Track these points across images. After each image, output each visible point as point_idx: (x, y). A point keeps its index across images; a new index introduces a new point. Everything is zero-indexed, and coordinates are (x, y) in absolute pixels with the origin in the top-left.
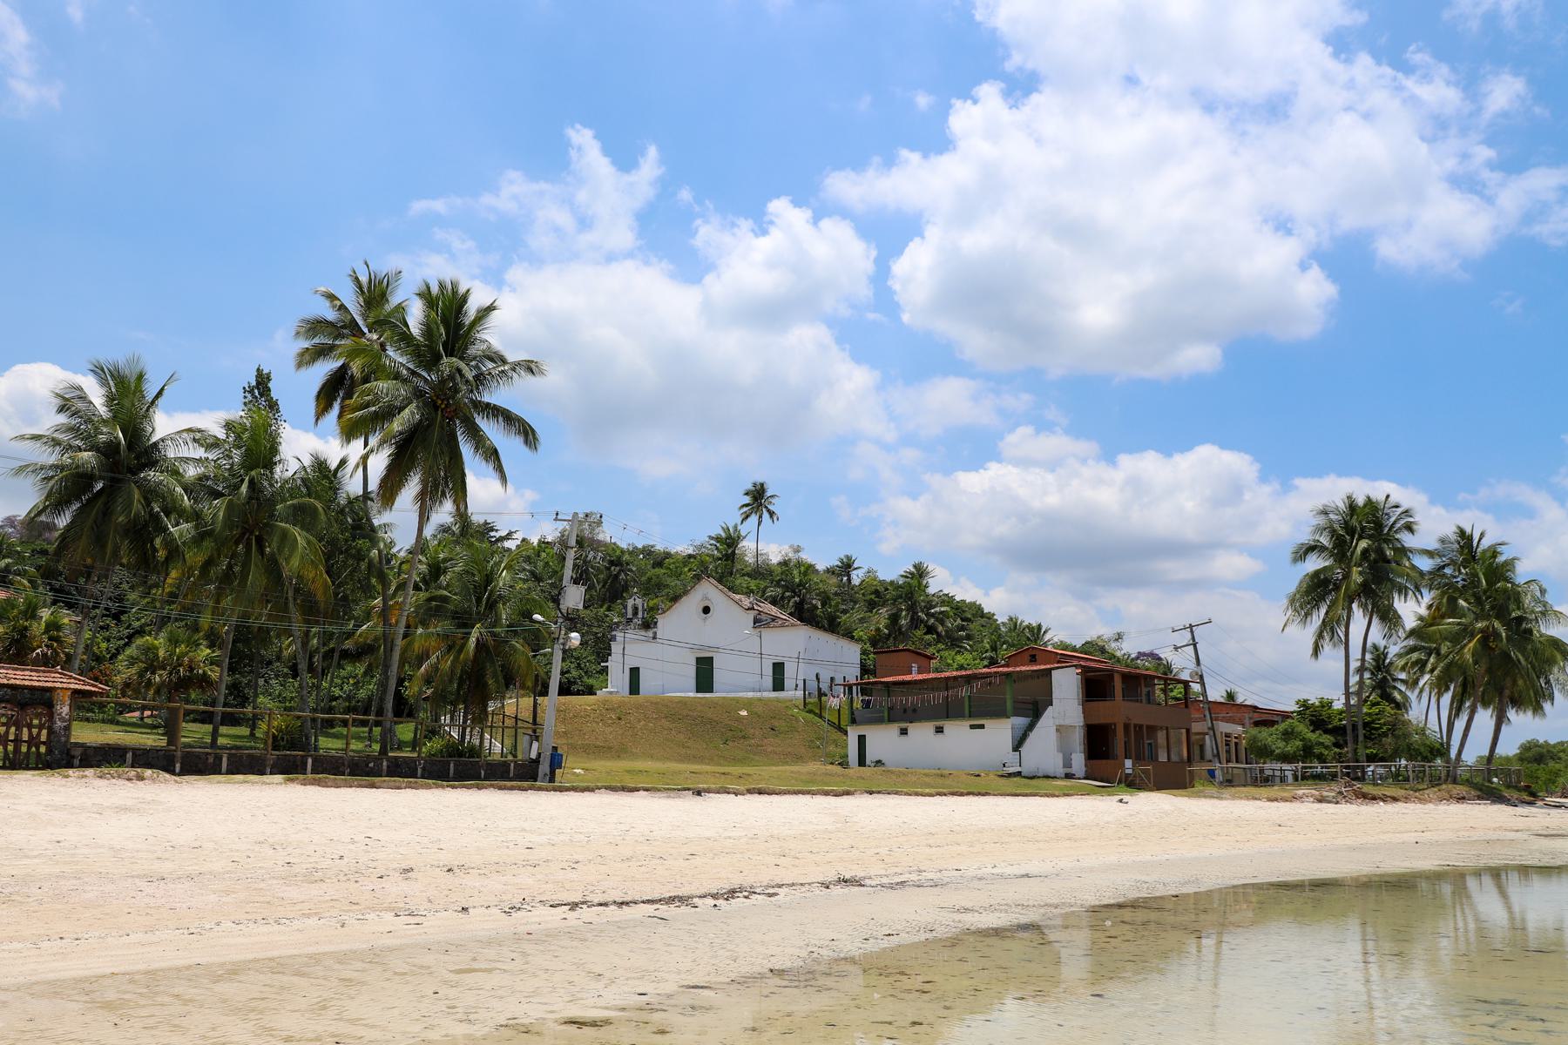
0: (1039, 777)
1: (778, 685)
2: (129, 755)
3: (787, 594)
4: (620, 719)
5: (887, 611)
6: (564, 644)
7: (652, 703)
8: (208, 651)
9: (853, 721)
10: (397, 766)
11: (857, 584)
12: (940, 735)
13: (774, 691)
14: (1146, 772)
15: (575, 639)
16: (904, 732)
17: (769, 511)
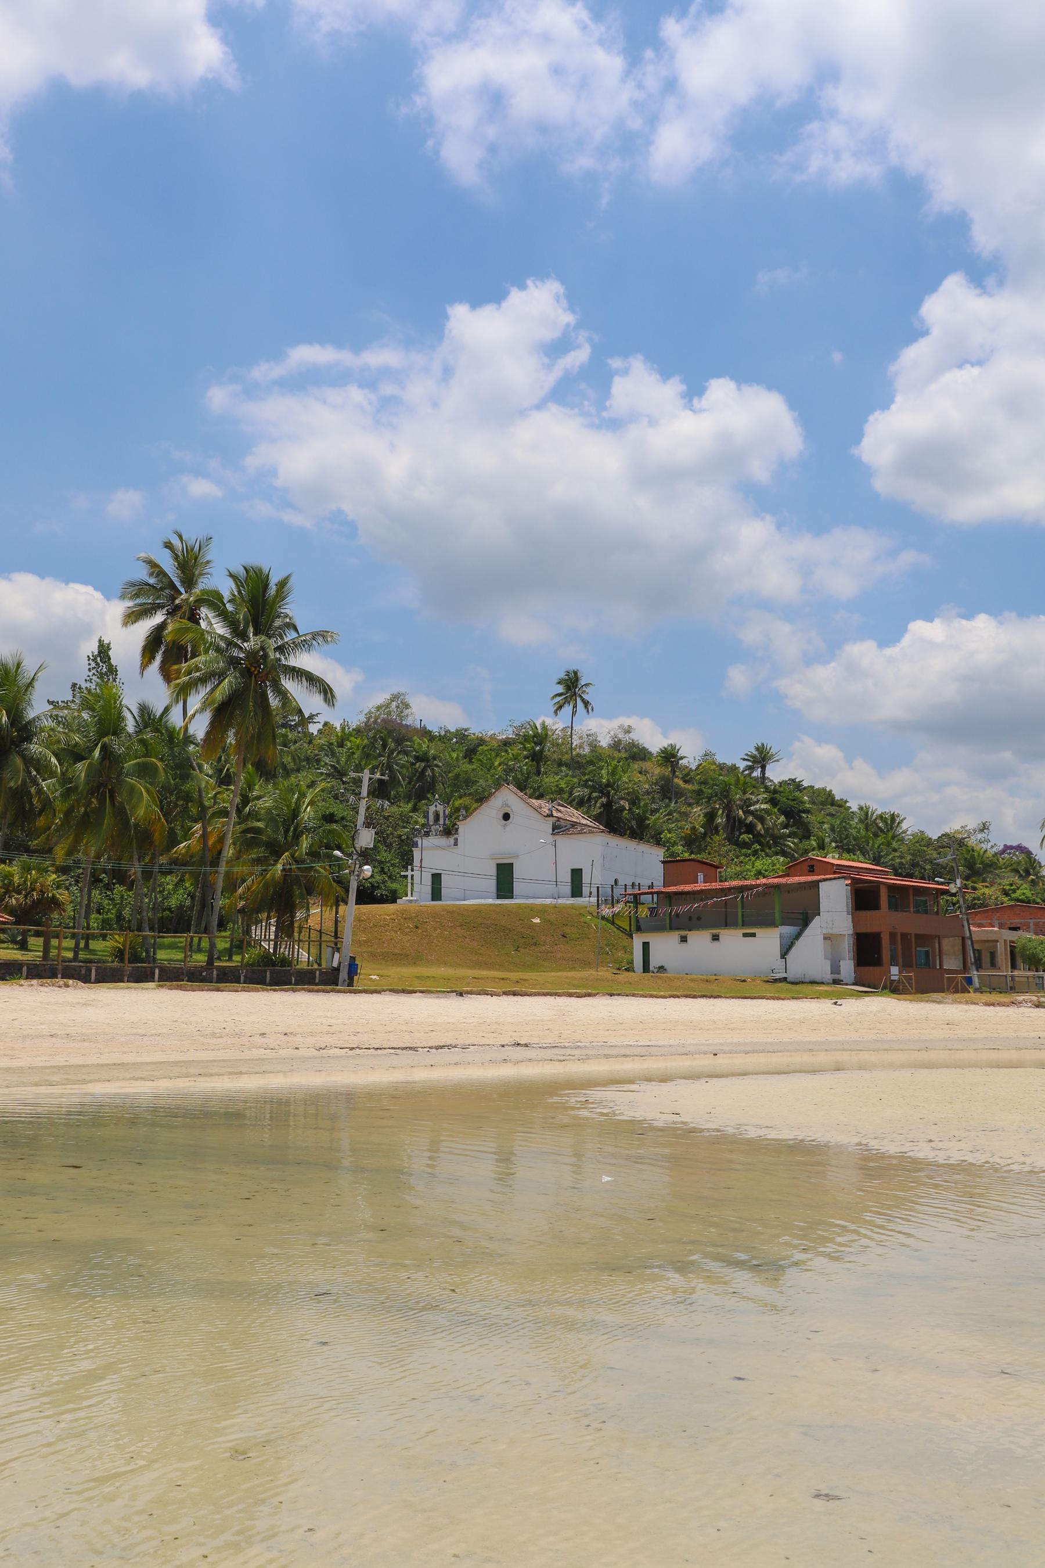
0: (803, 983)
1: (576, 890)
2: (25, 969)
3: (595, 795)
4: (417, 927)
5: (701, 810)
6: (358, 876)
7: (448, 912)
8: (54, 876)
9: (639, 929)
10: (225, 974)
11: (694, 768)
12: (684, 944)
13: (572, 897)
14: (909, 979)
15: (367, 870)
16: (684, 939)
17: (583, 700)
